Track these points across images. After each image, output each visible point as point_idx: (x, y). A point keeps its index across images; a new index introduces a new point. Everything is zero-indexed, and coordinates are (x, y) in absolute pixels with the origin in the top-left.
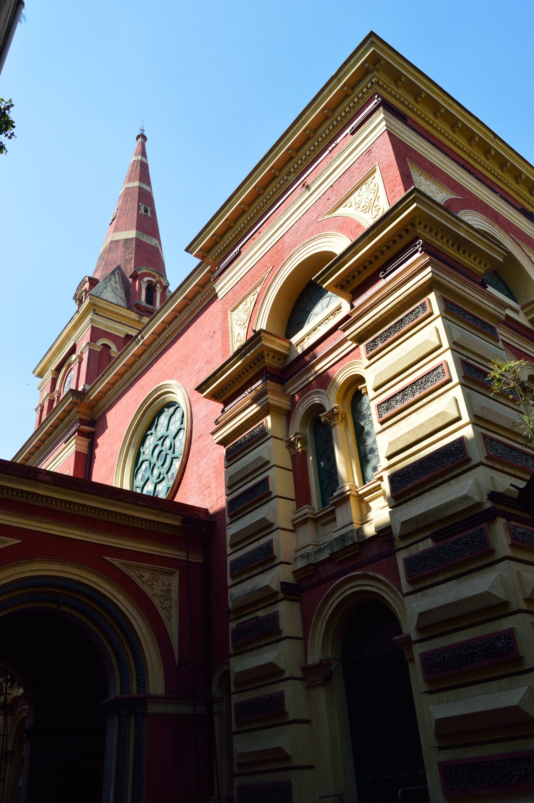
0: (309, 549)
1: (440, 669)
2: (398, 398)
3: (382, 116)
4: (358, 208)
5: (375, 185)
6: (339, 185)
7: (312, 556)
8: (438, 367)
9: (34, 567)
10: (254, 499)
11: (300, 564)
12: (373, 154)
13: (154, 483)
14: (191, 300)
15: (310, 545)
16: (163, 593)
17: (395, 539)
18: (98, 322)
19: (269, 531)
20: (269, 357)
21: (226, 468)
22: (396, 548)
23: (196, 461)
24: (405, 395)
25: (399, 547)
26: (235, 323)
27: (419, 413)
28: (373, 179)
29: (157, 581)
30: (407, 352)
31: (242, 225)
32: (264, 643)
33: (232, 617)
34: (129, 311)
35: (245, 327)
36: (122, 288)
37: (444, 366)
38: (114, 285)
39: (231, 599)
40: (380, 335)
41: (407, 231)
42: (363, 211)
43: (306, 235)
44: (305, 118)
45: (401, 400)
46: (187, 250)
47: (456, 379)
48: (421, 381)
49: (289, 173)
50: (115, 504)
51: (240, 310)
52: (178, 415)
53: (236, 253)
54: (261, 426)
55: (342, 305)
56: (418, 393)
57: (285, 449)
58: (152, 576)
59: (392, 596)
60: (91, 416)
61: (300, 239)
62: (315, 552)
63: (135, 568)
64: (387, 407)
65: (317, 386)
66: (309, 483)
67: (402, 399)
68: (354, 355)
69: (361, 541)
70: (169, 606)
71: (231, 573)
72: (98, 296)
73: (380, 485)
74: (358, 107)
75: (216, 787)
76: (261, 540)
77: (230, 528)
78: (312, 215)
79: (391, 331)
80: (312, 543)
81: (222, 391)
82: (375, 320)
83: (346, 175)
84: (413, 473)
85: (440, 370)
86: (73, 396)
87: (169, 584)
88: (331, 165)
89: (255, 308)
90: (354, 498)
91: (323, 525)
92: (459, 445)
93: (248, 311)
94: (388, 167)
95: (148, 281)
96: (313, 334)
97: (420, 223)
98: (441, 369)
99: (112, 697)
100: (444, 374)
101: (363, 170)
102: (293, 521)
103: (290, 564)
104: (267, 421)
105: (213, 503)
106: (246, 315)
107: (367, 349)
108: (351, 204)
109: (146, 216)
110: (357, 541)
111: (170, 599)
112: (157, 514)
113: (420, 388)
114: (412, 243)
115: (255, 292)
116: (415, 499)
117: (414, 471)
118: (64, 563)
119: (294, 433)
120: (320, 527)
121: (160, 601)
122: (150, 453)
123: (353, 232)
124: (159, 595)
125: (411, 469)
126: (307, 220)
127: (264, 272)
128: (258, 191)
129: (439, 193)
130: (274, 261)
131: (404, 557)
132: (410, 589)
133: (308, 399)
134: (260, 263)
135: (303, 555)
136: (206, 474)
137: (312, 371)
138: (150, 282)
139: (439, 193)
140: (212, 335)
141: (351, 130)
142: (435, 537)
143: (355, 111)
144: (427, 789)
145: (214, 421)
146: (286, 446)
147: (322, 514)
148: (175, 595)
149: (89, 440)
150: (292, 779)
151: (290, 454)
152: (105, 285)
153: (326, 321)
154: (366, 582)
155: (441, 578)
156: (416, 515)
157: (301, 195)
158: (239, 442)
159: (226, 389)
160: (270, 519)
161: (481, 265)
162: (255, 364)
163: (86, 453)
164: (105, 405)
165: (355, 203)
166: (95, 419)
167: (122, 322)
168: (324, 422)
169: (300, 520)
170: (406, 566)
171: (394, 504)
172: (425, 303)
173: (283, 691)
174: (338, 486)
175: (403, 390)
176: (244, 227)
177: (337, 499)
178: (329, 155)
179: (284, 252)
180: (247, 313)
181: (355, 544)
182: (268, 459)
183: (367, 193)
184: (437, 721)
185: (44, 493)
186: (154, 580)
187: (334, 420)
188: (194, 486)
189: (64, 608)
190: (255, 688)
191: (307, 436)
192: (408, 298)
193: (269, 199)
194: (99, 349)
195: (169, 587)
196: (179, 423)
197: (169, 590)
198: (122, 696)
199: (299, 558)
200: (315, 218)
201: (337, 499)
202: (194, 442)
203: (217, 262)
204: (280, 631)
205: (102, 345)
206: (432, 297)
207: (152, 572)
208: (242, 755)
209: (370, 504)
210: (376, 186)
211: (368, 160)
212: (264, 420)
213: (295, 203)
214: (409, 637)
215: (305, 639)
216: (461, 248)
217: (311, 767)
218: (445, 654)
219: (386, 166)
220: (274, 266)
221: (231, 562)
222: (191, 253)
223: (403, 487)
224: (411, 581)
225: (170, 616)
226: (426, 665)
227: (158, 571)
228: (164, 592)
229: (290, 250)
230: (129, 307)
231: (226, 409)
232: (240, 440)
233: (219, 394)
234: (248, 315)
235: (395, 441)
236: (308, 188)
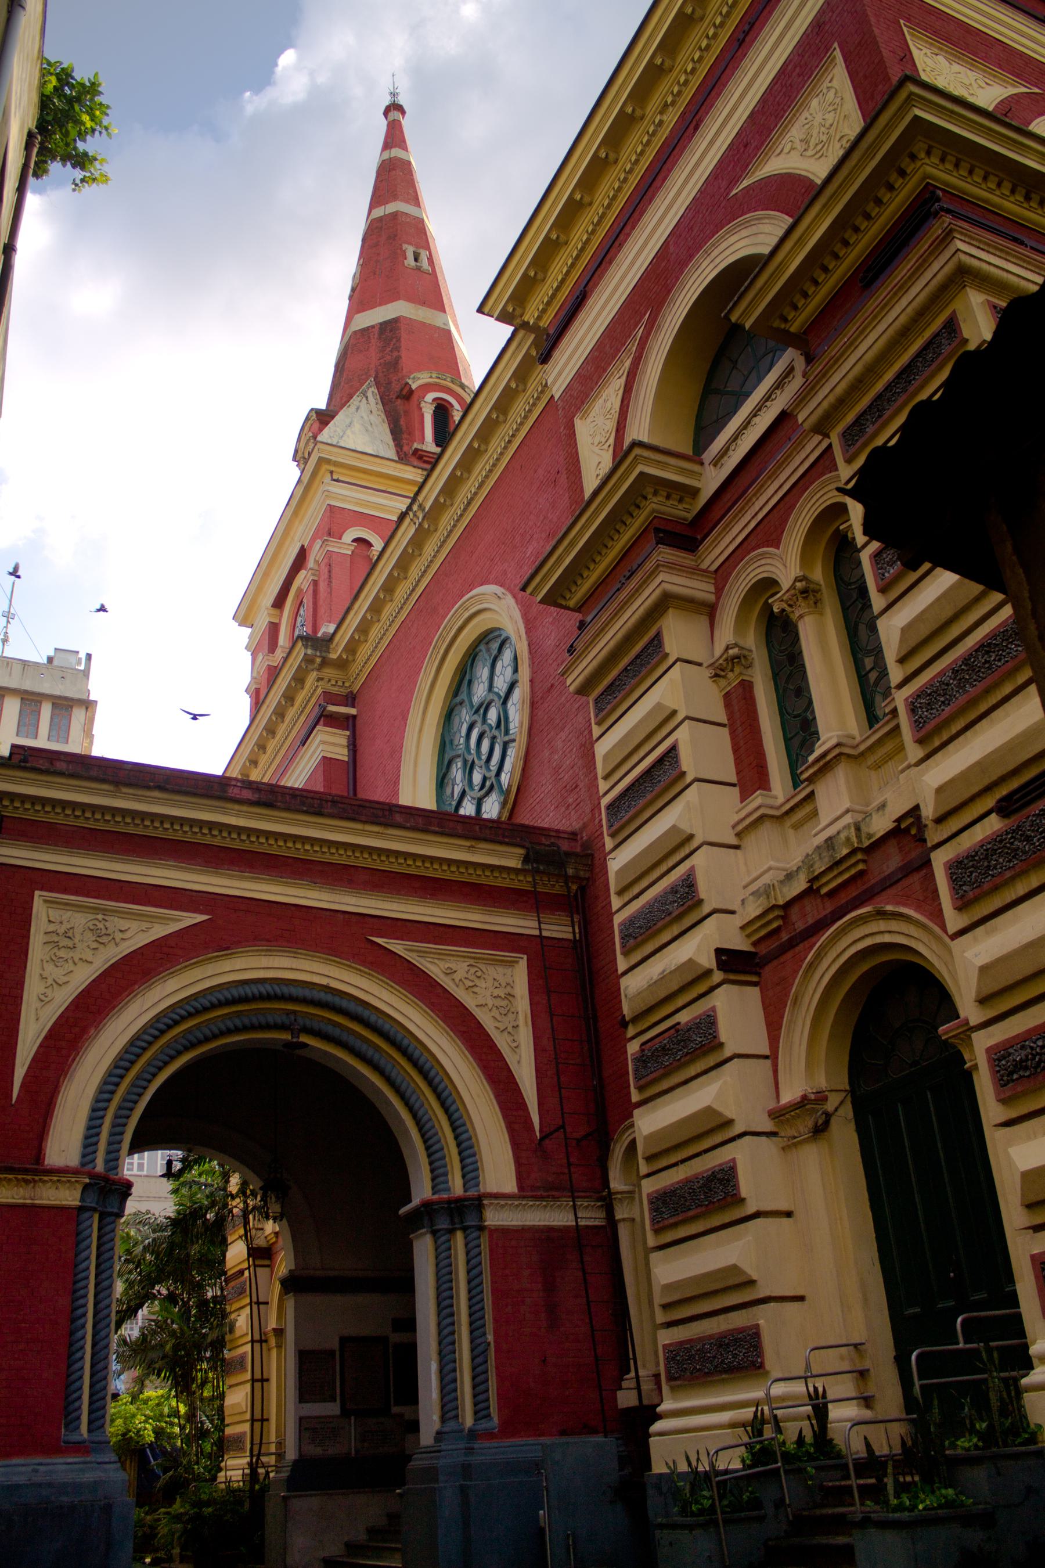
0: (766, 879)
1: (1027, 1074)
7: (774, 889)
10: (654, 793)
11: (753, 910)
13: (474, 799)
17: (926, 826)
18: (340, 497)
23: (546, 740)
25: (936, 841)
29: (484, 979)
32: (692, 1071)
33: (631, 1031)
34: (399, 466)
36: (383, 421)
38: (366, 418)
39: (626, 996)
46: (480, 310)
52: (507, 656)
55: (796, 364)
57: (710, 681)
58: (473, 970)
60: (347, 684)
62: (781, 882)
63: (436, 956)
69: (867, 844)
70: (513, 1027)
71: (623, 946)
72: (334, 443)
75: (631, 1356)
76: (673, 872)
86: (306, 647)
95: (435, 400)
99: (416, 1202)
103: (733, 912)
105: (585, 820)
109: (419, 269)
115: (621, 372)
116: (961, 738)
118: (295, 953)
120: (791, 832)
122: (462, 741)
124: (490, 1006)
129: (982, 88)
131: (946, 859)
135: (758, 890)
136: (568, 762)
138: (439, 402)
139: (982, 88)
142: (1004, 808)
144: (1018, 1317)
148: (523, 1004)
149: (348, 733)
150: (761, 1322)
152: (348, 421)
153: (768, 404)
160: (686, 827)
161: (1032, 204)
163: (346, 759)
166: (355, 692)
167: (389, 490)
170: (951, 878)
173: (734, 1160)
174: (819, 739)
181: (853, 852)
184: (1025, 1175)
185: (242, 822)
186: (479, 977)
188: (546, 791)
189: (304, 1039)
190: (683, 1161)
193: (631, 171)
194: (348, 549)
195: (509, 990)
196: (509, 671)
197: (509, 994)
198: (436, 1197)
199: (751, 897)
200: (723, 190)
202: (539, 704)
205: (355, 540)
207: (472, 962)
208: (668, 1287)
214: (967, 1022)
215: (773, 1057)
216: (1033, 196)
217: (801, 1298)
218: (1035, 1043)
221: (620, 925)
223: (934, 717)
224: (962, 905)
225: (515, 1044)
226: (998, 1069)
230: (403, 458)
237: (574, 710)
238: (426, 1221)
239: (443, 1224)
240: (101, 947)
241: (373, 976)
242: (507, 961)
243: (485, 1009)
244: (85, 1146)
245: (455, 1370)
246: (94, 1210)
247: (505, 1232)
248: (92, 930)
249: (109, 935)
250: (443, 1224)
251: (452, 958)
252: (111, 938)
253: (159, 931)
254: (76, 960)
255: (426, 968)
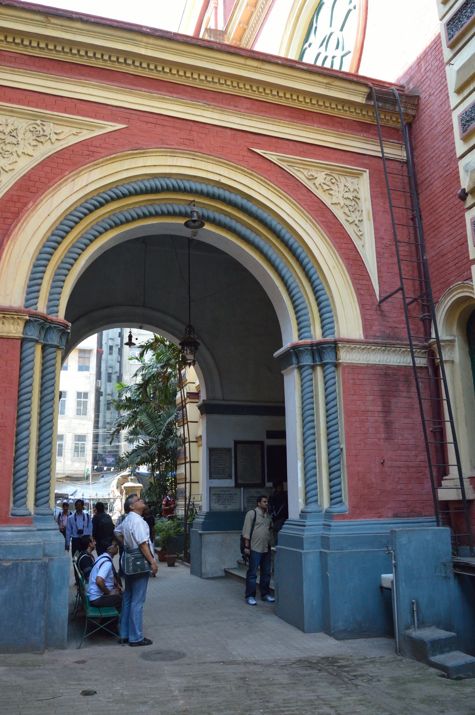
9: (150, 161)
16: (348, 202)
29: (337, 185)
50: (260, 68)
58: (329, 178)
63: (301, 166)
70: (359, 221)
87: (355, 190)
99: (287, 345)
105: (411, 74)
111: (359, 211)
112: (326, 84)
118: (194, 155)
121: (344, 213)
124: (342, 205)
164: (249, 41)
195: (355, 194)
197: (356, 197)
198: (302, 342)
207: (328, 172)
225: (361, 233)
227: (337, 170)
228: (348, 200)
238: (294, 360)
239: (307, 360)
240: (40, 145)
241: (254, 176)
242: (354, 173)
243: (338, 206)
244: (28, 293)
245: (315, 468)
246: (37, 341)
247: (354, 368)
248: (32, 132)
249: (47, 136)
250: (307, 360)
251: (313, 168)
252: (47, 138)
253: (86, 135)
254: (20, 153)
255: (295, 174)
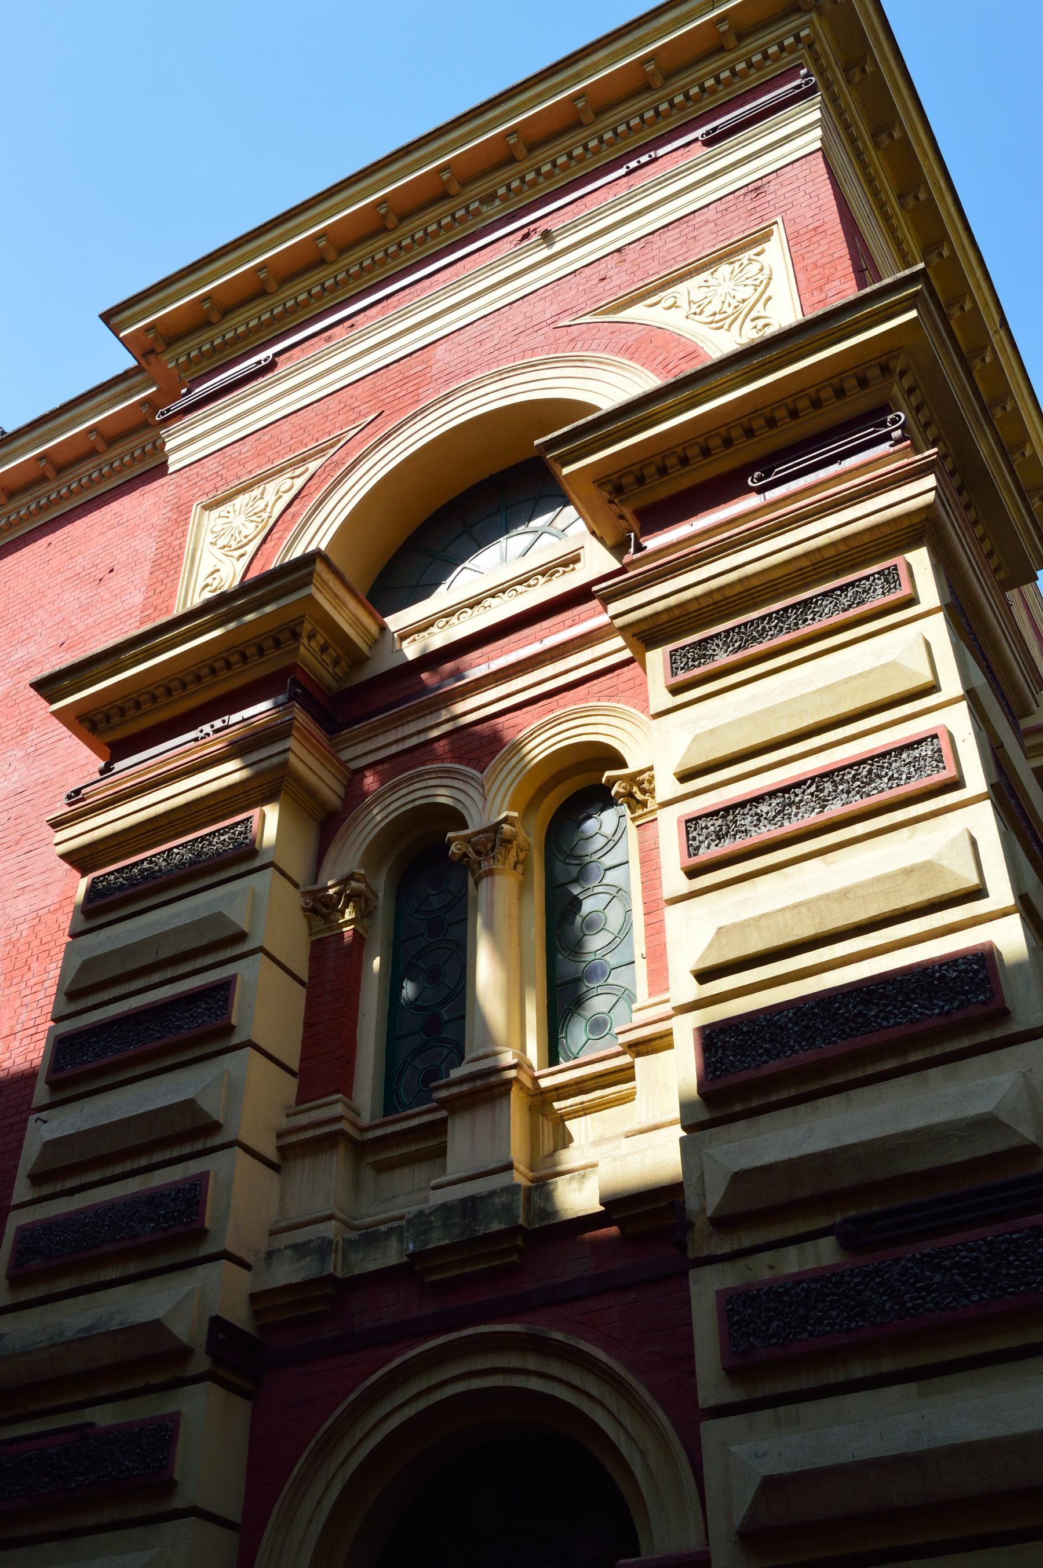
0: (329, 1230)
2: (764, 808)
3: (817, 115)
4: (695, 314)
5: (761, 270)
6: (645, 251)
8: (920, 742)
12: (769, 198)
14: (61, 469)
15: (330, 1217)
17: (692, 1225)
19: (199, 1146)
20: (313, 643)
21: (74, 935)
22: (691, 1254)
24: (790, 805)
25: (705, 1252)
26: (210, 538)
27: (834, 862)
28: (757, 254)
30: (821, 684)
31: (303, 297)
35: (243, 555)
37: (944, 743)
40: (725, 631)
41: (863, 383)
42: (712, 322)
43: (509, 354)
44: (587, 68)
45: (775, 817)
46: (107, 317)
47: (976, 781)
48: (853, 772)
49: (491, 197)
51: (237, 507)
53: (259, 362)
54: (239, 828)
56: (838, 803)
57: (300, 914)
59: (626, 1419)
61: (486, 359)
64: (721, 830)
65: (449, 755)
66: (354, 1031)
67: (779, 813)
68: (596, 689)
69: (537, 1226)
73: (631, 1067)
74: (740, 87)
77: (45, 1122)
78: (539, 309)
79: (764, 628)
80: (338, 1214)
81: (122, 711)
82: (720, 589)
83: (673, 233)
84: (792, 1028)
85: (926, 750)
88: (630, 198)
89: (292, 510)
90: (522, 1095)
91: (381, 1168)
92: (975, 967)
93: (265, 515)
94: (813, 233)
96: (464, 615)
97: (902, 374)
98: (931, 747)
100: (941, 765)
101: (731, 228)
102: (280, 1135)
104: (263, 816)
106: (255, 524)
107: (672, 664)
108: (676, 302)
110: (524, 1225)
113: (848, 792)
114: (876, 415)
117: (795, 1024)
119: (343, 871)
120: (368, 1173)
123: (670, 366)
125: (786, 1016)
126: (521, 317)
127: (346, 424)
128: (384, 216)
130: (387, 401)
131: (719, 1286)
132: (730, 1395)
133: (411, 788)
134: (338, 398)
137: (443, 712)
140: (100, 576)
141: (708, 133)
143: (730, 93)
145: (69, 792)
146: (303, 908)
147: (380, 1132)
151: (310, 935)
154: (532, 1363)
155: (858, 1371)
156: (794, 1154)
157: (515, 256)
158: (146, 865)
159: (138, 705)
160: (213, 1107)
162: (261, 651)
165: (690, 302)
168: (456, 859)
169: (310, 1134)
171: (704, 1116)
172: (896, 569)
175: (786, 790)
176: (306, 304)
177: (465, 1088)
178: (625, 180)
179: (424, 383)
180: (259, 520)
181: (515, 1230)
182: (246, 928)
183: (733, 283)
187: (493, 858)
191: (376, 896)
192: (842, 548)
193: (408, 249)
199: (288, 1253)
201: (465, 1088)
203: (188, 377)
204: (169, 1486)
206: (920, 559)
209: (573, 1126)
210: (766, 271)
211: (749, 207)
212: (255, 812)
213: (492, 269)
219: (805, 230)
220: (383, 415)
221: (20, 1230)
222: (115, 331)
223: (747, 1068)
229: (447, 383)
231: (118, 766)
232: (150, 860)
233: (108, 718)
234: (260, 526)
235: (739, 927)
236: (547, 237)
237: (14, 888)
